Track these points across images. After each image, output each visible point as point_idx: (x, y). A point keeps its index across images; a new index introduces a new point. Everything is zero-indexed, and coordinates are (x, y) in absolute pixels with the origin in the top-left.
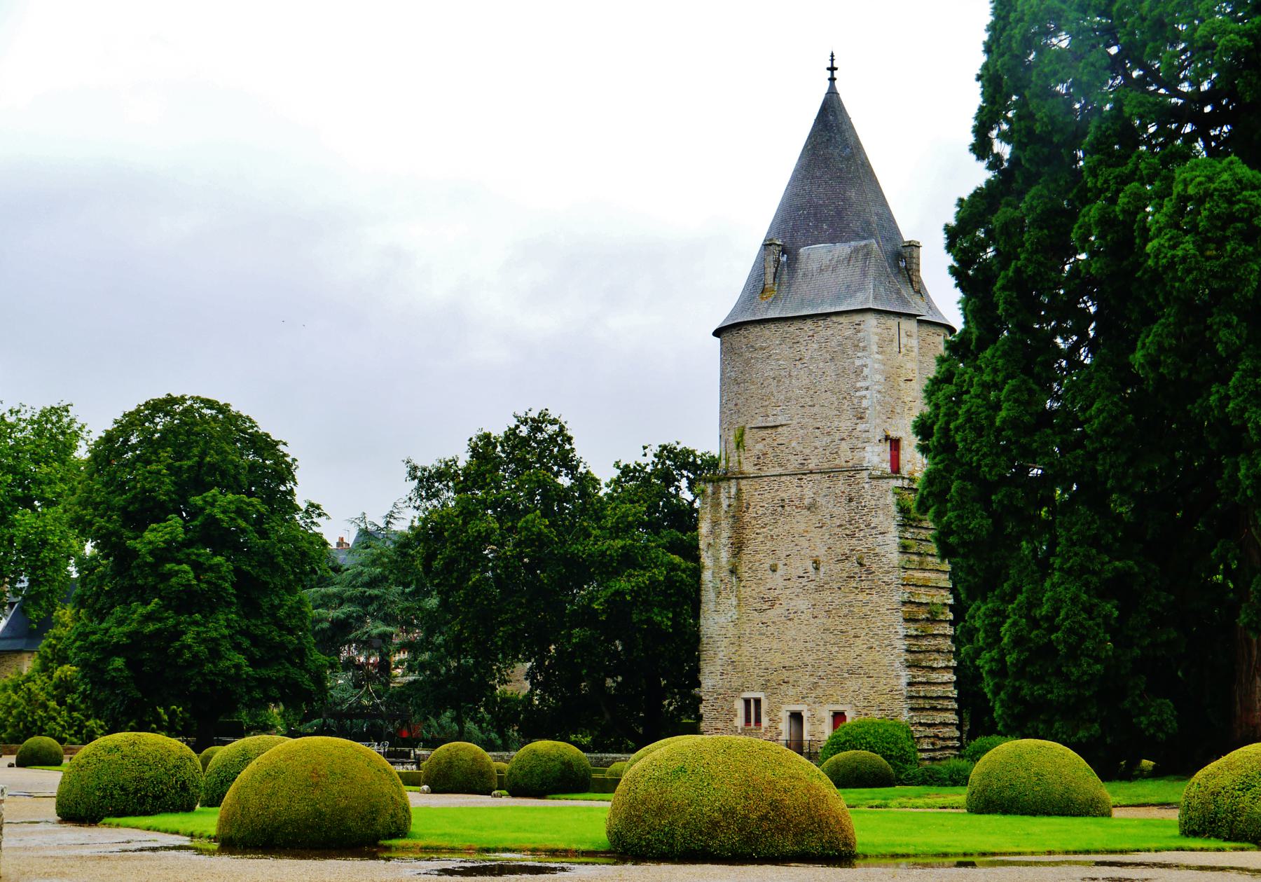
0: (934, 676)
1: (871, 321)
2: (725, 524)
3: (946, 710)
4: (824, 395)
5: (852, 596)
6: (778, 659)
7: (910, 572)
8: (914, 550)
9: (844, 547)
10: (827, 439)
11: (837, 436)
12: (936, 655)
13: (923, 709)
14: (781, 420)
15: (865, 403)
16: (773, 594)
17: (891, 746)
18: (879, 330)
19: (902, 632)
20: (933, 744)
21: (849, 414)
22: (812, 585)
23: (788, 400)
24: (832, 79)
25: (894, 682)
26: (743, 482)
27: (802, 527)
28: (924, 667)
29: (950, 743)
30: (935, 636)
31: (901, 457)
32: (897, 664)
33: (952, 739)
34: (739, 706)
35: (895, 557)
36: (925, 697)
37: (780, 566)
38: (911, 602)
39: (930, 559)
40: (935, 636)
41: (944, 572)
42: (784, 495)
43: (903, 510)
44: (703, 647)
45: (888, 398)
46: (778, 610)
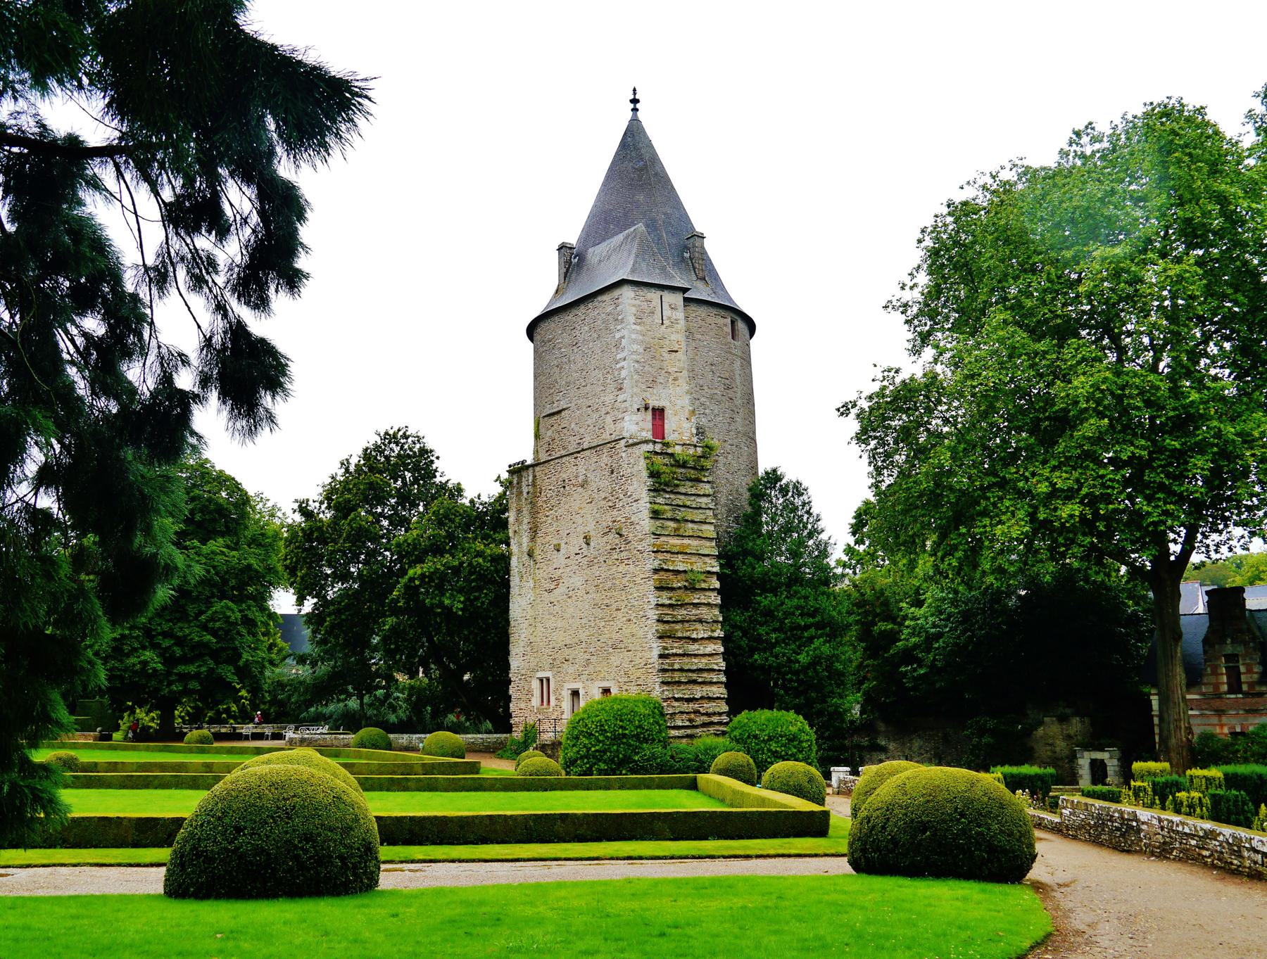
0: (693, 648)
1: (627, 293)
2: (525, 512)
3: (711, 683)
4: (594, 374)
5: (614, 568)
6: (560, 638)
7: (662, 539)
8: (669, 515)
9: (607, 520)
10: (595, 416)
11: (603, 411)
12: (698, 626)
13: (679, 683)
14: (563, 405)
15: (624, 373)
16: (558, 572)
17: (625, 724)
18: (638, 302)
19: (654, 601)
20: (690, 720)
21: (612, 387)
22: (585, 561)
23: (568, 384)
24: (635, 110)
25: (647, 655)
26: (537, 469)
27: (575, 506)
28: (680, 638)
29: (715, 719)
30: (696, 605)
31: (666, 426)
32: (650, 636)
33: (720, 714)
34: (535, 685)
35: (647, 524)
36: (681, 670)
37: (563, 545)
38: (662, 569)
39: (690, 525)
40: (696, 605)
41: (710, 539)
42: (564, 476)
43: (654, 474)
44: (512, 630)
45: (647, 368)
46: (562, 589)
